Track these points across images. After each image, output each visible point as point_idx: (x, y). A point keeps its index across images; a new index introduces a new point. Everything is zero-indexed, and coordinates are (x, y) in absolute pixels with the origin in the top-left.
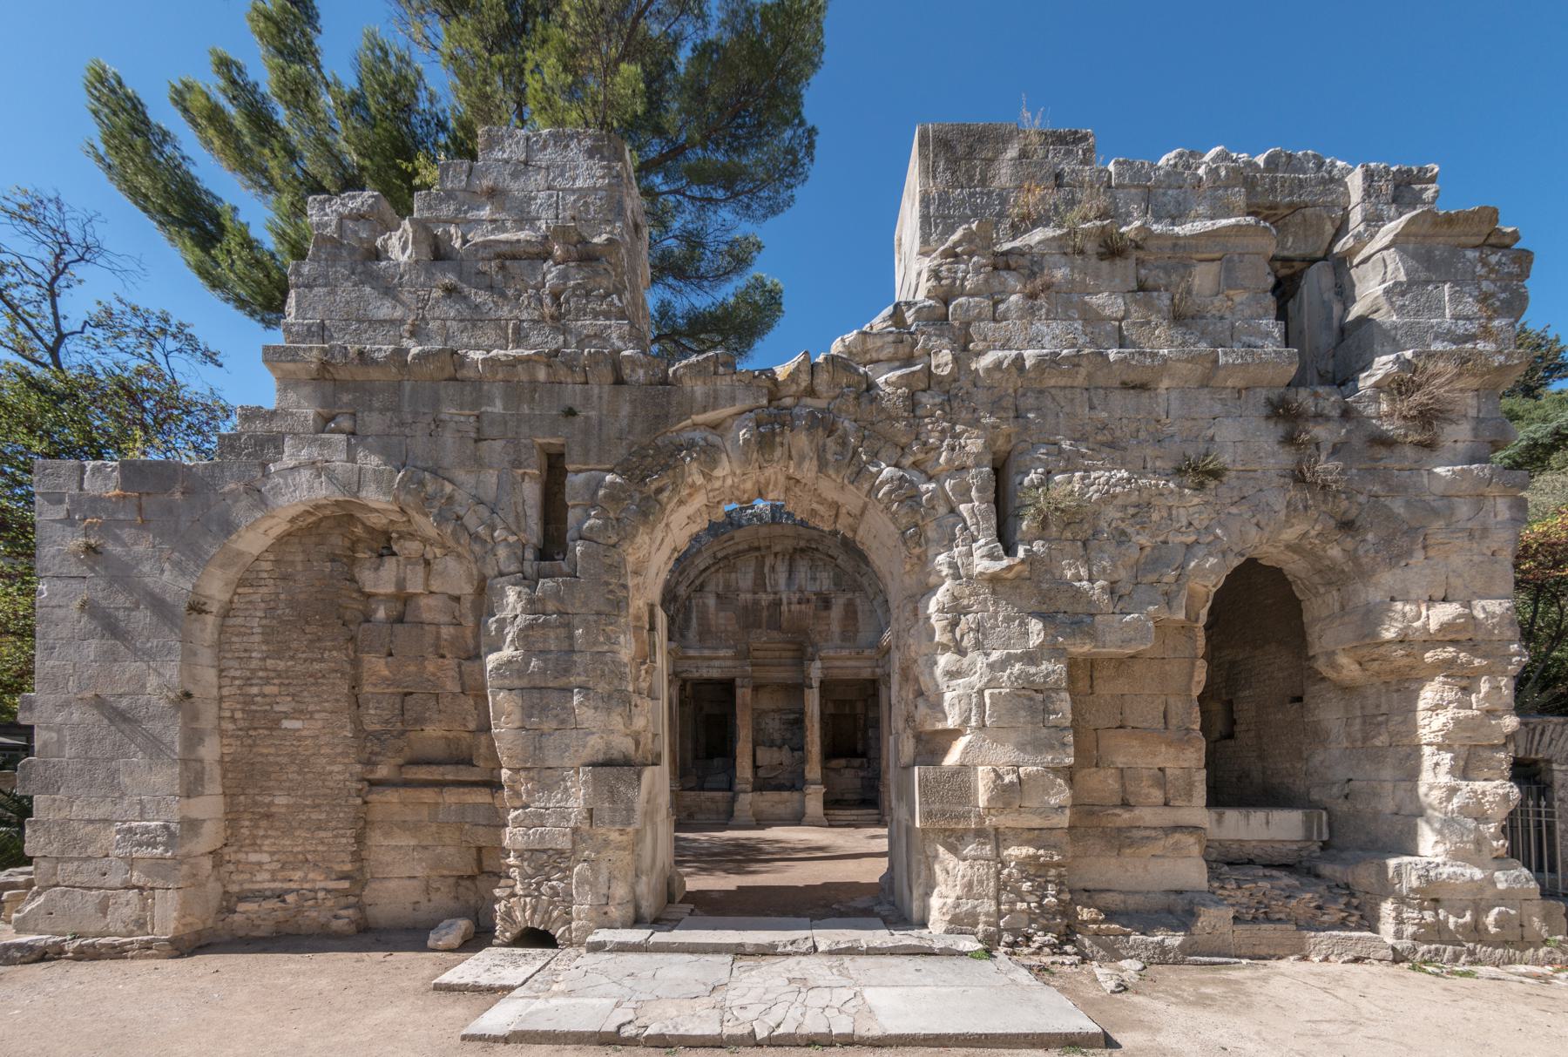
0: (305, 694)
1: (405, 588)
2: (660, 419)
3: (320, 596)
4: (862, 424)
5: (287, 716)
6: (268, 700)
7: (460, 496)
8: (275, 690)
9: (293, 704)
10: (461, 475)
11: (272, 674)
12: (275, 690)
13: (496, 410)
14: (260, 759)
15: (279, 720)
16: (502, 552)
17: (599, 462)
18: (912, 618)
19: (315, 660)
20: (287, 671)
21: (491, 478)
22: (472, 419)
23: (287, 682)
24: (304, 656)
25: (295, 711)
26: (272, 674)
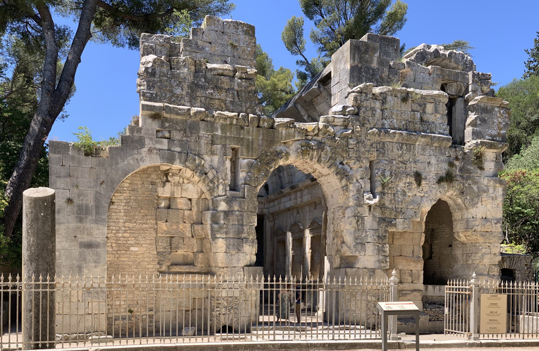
0: (140, 237)
1: (174, 195)
2: (272, 142)
3: (147, 198)
4: (332, 148)
5: (132, 245)
6: (125, 239)
7: (207, 166)
8: (128, 235)
9: (135, 241)
10: (206, 157)
11: (127, 229)
12: (128, 235)
13: (218, 134)
14: (121, 263)
15: (129, 247)
16: (221, 187)
17: (252, 156)
18: (342, 216)
19: (144, 223)
20: (133, 228)
21: (216, 159)
22: (210, 136)
23: (133, 232)
24: (140, 222)
25: (136, 243)
26: (127, 229)
